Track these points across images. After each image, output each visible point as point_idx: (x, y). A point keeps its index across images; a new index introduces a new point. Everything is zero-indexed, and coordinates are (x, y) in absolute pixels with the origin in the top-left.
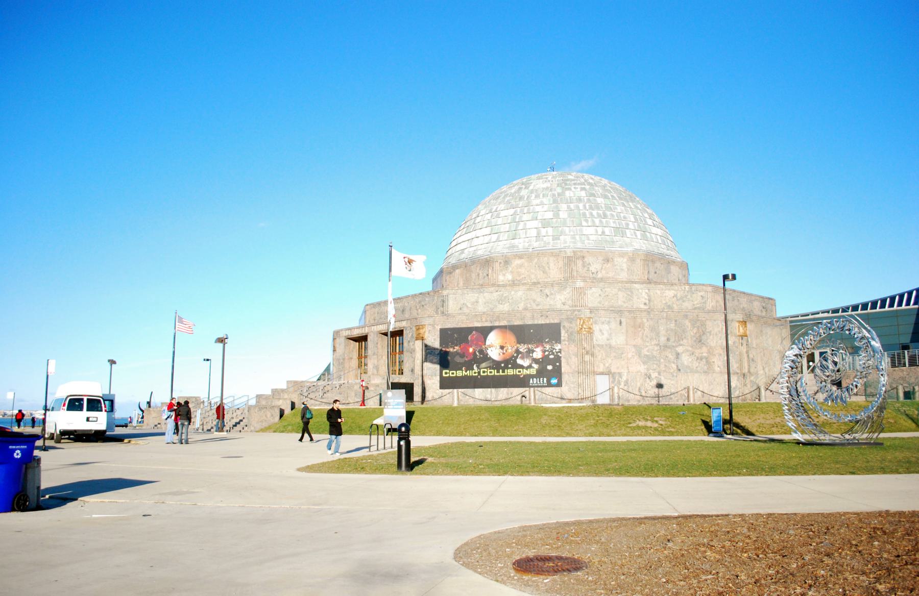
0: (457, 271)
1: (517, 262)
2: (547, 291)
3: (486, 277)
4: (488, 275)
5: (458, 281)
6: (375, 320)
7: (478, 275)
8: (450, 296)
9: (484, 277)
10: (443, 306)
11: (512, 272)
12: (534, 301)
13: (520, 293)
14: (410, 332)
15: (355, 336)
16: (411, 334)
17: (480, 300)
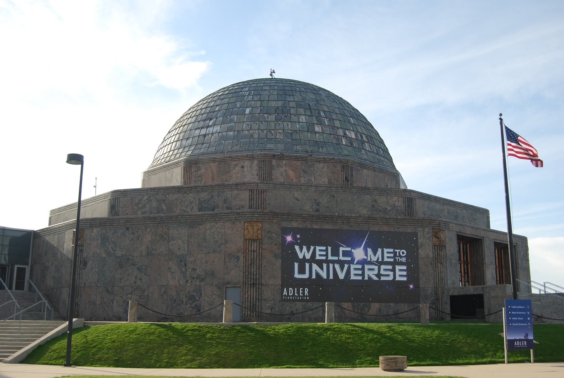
0: (365, 171)
5: (366, 181)
6: (425, 214)
15: (468, 236)
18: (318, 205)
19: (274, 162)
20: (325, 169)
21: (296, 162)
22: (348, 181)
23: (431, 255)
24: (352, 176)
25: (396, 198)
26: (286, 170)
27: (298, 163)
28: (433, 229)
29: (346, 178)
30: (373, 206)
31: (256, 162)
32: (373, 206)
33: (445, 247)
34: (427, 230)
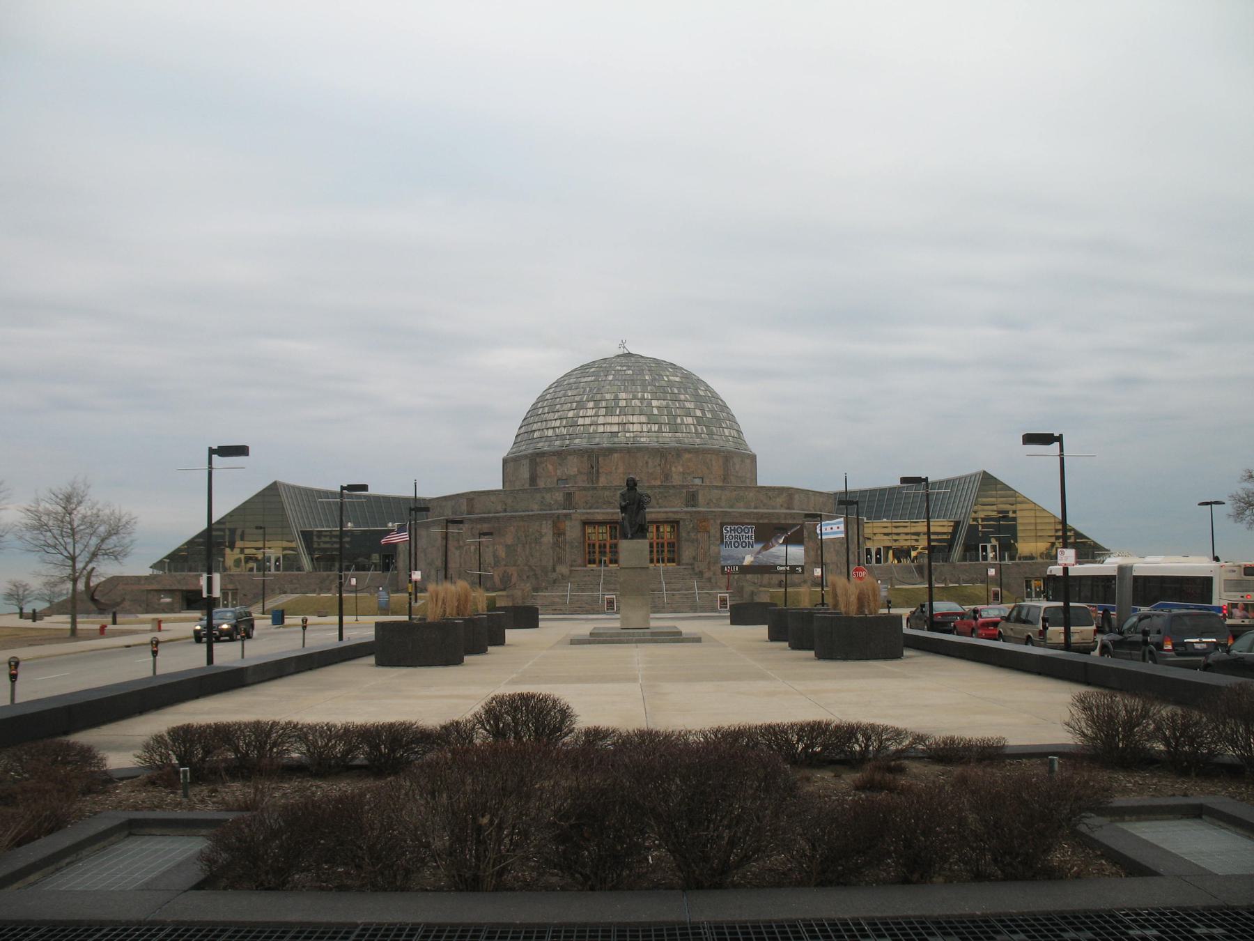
1: (687, 456)
2: (770, 494)
3: (658, 468)
4: (660, 465)
5: (617, 465)
6: (587, 503)
7: (647, 463)
8: (700, 491)
9: (655, 467)
10: (693, 500)
11: (683, 465)
12: (762, 502)
13: (751, 494)
14: (690, 524)
16: (691, 525)
17: (723, 497)
18: (506, 505)
19: (538, 460)
20: (575, 460)
21: (553, 457)
22: (592, 467)
23: (551, 541)
24: (598, 462)
25: (557, 494)
26: (546, 466)
27: (555, 458)
28: (553, 521)
29: (591, 466)
30: (542, 502)
31: (528, 461)
32: (542, 502)
33: (564, 534)
34: (549, 522)
